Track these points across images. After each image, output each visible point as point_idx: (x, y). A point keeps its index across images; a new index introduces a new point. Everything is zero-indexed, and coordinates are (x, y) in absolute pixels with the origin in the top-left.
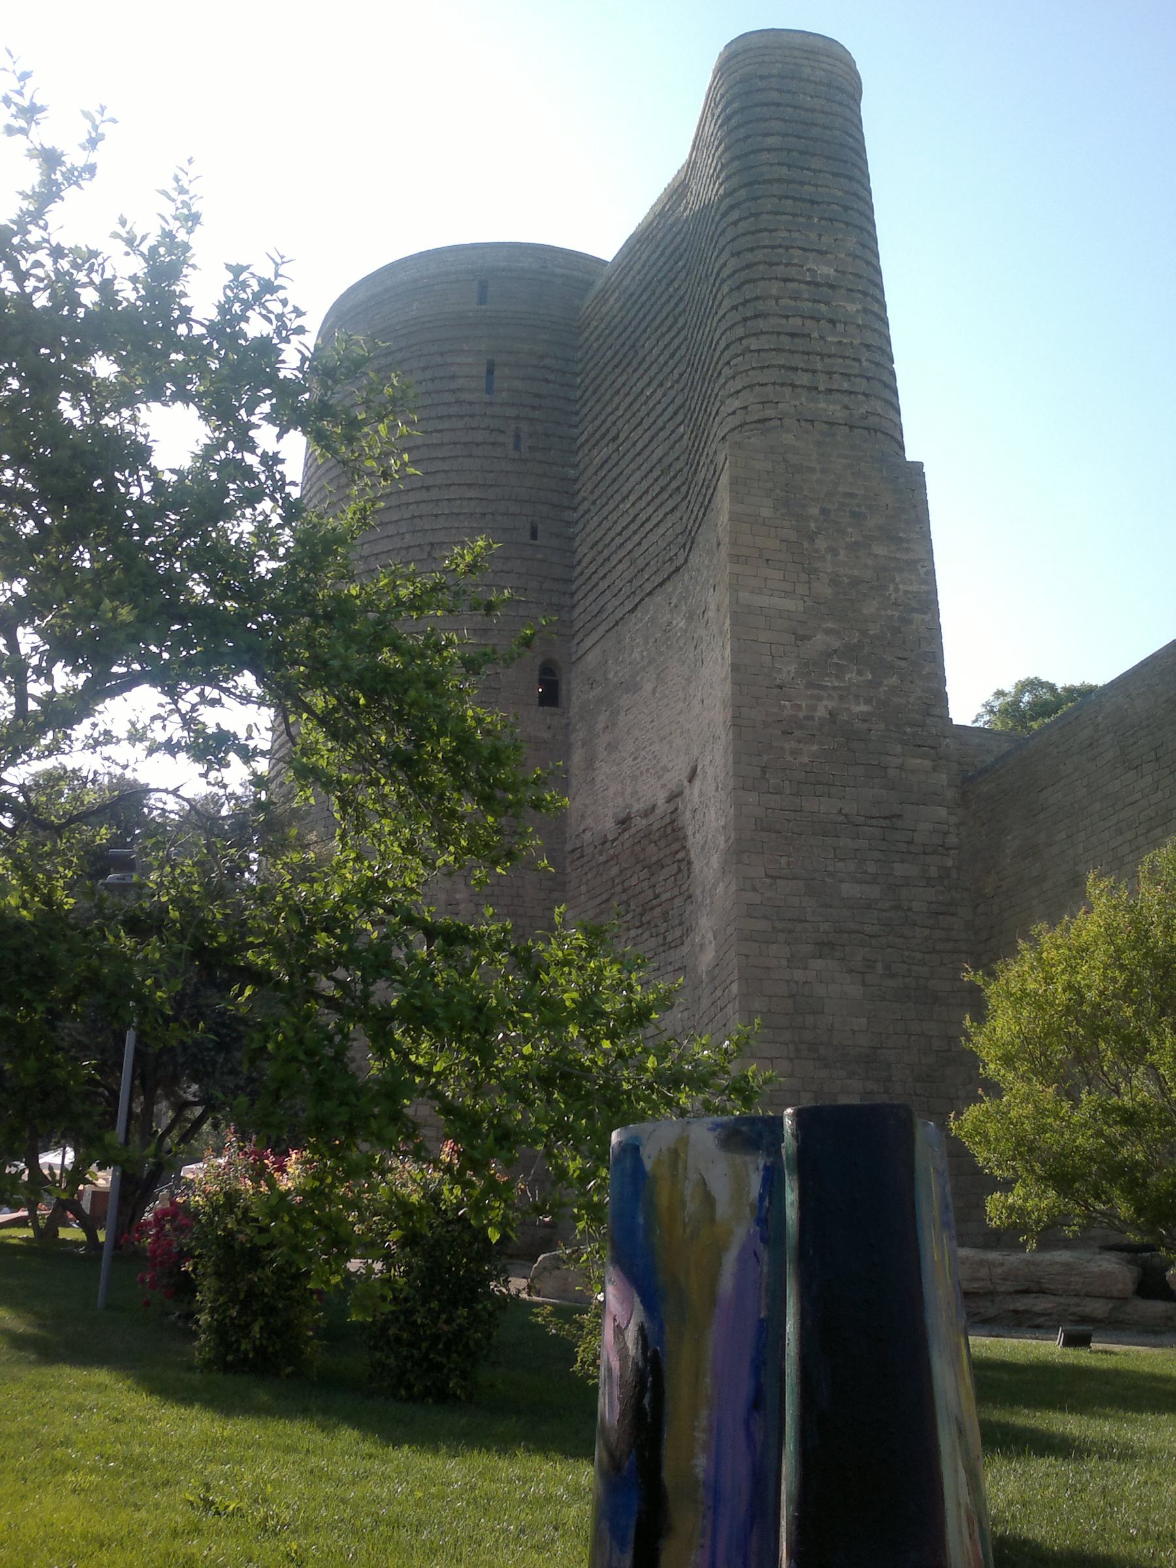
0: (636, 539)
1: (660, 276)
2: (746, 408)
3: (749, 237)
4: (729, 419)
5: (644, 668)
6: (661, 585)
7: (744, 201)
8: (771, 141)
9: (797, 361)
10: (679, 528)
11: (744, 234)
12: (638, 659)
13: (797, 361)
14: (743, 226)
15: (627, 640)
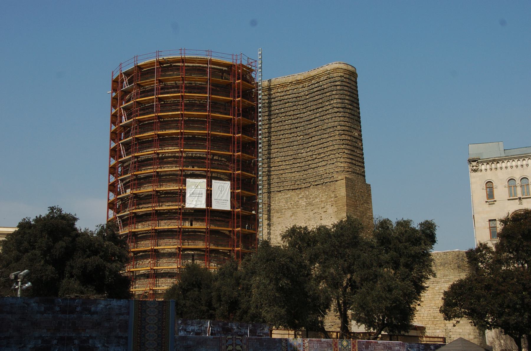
0: (281, 172)
1: (289, 100)
2: (344, 167)
3: (343, 122)
4: (340, 168)
5: (286, 209)
6: (293, 190)
7: (342, 112)
8: (347, 97)
9: (353, 158)
10: (301, 177)
11: (342, 121)
12: (283, 206)
13: (353, 158)
14: (342, 119)
15: (277, 199)
